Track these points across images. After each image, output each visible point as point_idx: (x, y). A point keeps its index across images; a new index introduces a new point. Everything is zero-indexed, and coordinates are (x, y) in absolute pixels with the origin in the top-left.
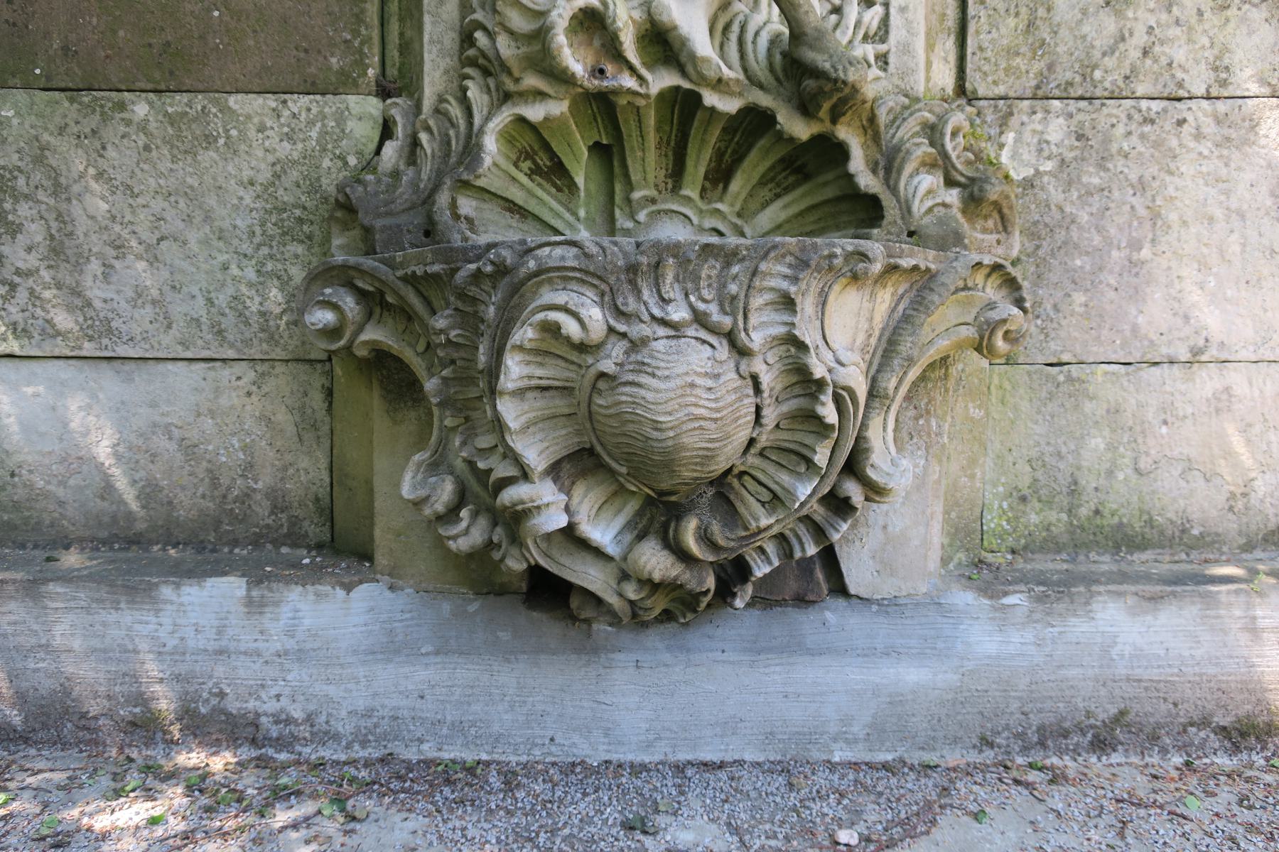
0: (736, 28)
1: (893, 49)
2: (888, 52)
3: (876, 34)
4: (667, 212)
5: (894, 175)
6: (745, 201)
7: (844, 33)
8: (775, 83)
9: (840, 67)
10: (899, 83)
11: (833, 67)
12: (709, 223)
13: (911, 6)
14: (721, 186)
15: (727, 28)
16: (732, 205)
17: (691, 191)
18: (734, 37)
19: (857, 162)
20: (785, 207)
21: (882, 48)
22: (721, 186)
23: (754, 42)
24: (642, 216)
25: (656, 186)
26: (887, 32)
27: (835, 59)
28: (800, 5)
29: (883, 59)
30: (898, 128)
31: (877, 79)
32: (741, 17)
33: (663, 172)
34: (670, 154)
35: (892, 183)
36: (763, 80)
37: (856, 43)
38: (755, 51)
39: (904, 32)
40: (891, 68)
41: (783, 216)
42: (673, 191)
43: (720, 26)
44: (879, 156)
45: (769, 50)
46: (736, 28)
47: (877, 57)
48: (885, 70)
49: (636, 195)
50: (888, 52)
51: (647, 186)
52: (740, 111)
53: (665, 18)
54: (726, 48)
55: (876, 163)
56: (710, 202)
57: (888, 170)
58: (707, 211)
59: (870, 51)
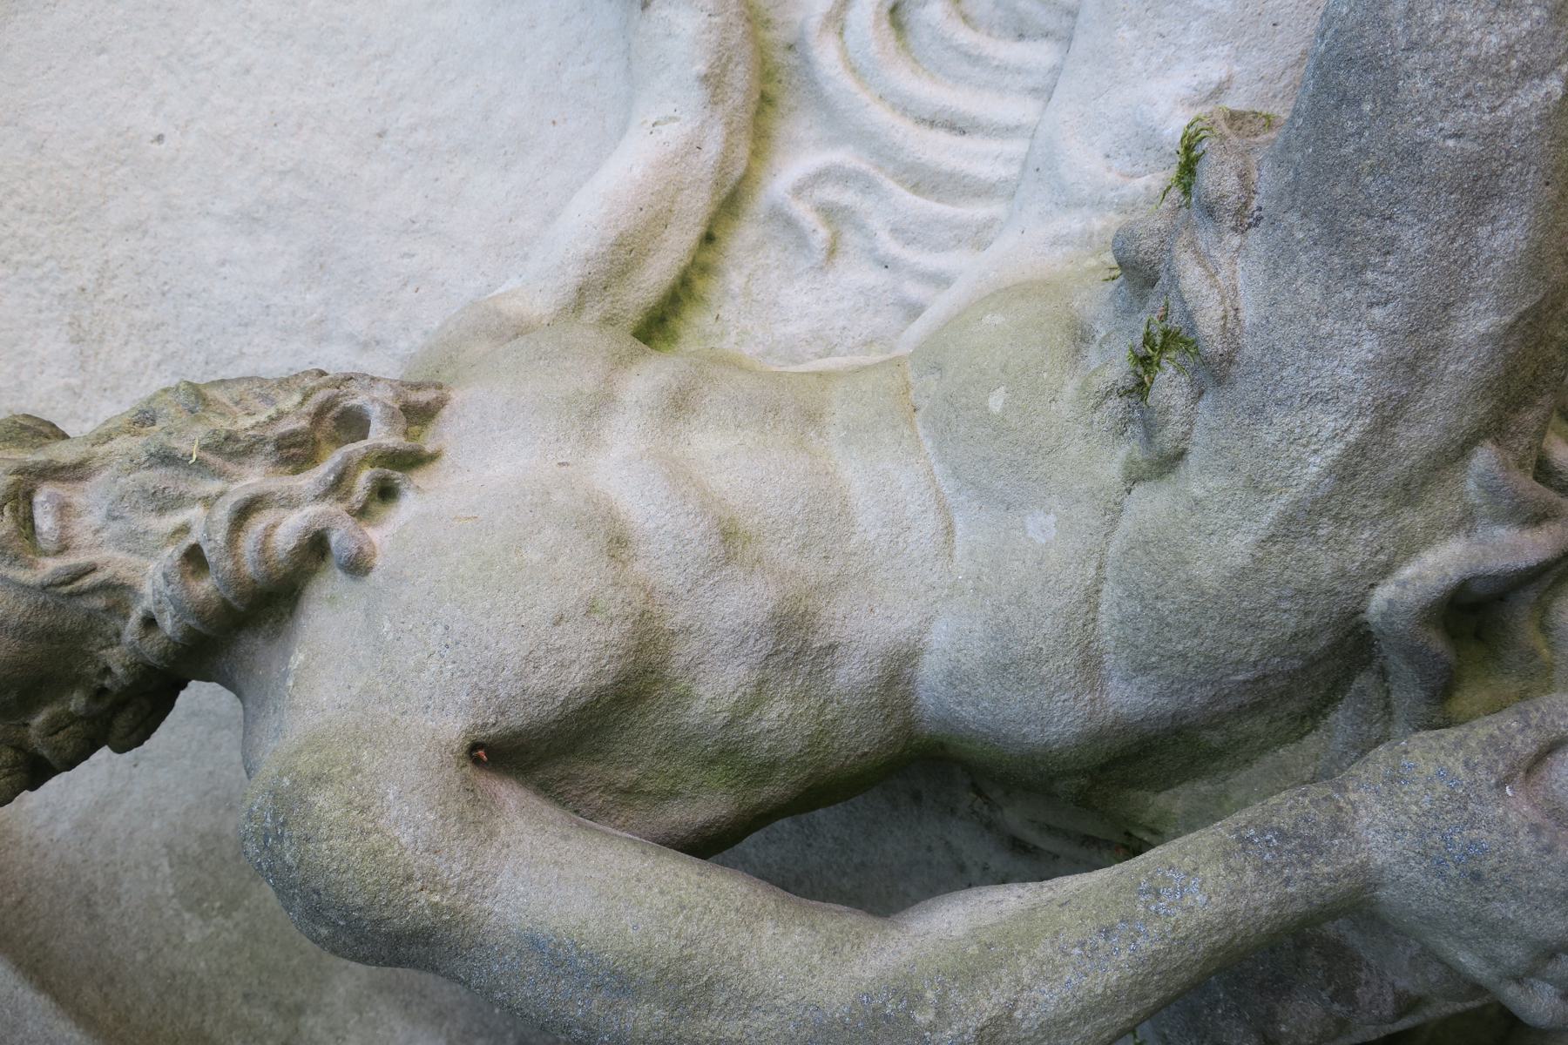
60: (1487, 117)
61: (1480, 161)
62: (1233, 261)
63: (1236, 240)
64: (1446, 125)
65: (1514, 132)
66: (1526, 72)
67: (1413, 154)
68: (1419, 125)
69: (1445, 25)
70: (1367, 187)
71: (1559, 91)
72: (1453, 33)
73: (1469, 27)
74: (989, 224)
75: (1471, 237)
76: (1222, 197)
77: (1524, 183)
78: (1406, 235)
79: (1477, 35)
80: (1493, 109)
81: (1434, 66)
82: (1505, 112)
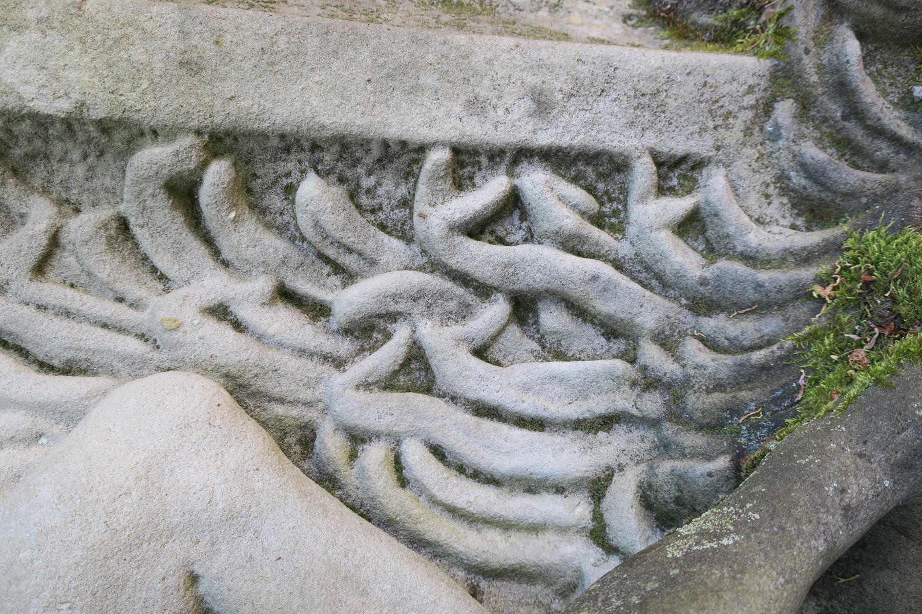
1: (651, 139)
3: (590, 190)
7: (607, 289)
10: (738, 125)
13: (530, 80)
21: (643, 173)
29: (675, 171)
30: (878, 132)
37: (624, 249)
39: (603, 105)
40: (700, 146)
47: (662, 190)
48: (700, 164)
59: (652, 214)
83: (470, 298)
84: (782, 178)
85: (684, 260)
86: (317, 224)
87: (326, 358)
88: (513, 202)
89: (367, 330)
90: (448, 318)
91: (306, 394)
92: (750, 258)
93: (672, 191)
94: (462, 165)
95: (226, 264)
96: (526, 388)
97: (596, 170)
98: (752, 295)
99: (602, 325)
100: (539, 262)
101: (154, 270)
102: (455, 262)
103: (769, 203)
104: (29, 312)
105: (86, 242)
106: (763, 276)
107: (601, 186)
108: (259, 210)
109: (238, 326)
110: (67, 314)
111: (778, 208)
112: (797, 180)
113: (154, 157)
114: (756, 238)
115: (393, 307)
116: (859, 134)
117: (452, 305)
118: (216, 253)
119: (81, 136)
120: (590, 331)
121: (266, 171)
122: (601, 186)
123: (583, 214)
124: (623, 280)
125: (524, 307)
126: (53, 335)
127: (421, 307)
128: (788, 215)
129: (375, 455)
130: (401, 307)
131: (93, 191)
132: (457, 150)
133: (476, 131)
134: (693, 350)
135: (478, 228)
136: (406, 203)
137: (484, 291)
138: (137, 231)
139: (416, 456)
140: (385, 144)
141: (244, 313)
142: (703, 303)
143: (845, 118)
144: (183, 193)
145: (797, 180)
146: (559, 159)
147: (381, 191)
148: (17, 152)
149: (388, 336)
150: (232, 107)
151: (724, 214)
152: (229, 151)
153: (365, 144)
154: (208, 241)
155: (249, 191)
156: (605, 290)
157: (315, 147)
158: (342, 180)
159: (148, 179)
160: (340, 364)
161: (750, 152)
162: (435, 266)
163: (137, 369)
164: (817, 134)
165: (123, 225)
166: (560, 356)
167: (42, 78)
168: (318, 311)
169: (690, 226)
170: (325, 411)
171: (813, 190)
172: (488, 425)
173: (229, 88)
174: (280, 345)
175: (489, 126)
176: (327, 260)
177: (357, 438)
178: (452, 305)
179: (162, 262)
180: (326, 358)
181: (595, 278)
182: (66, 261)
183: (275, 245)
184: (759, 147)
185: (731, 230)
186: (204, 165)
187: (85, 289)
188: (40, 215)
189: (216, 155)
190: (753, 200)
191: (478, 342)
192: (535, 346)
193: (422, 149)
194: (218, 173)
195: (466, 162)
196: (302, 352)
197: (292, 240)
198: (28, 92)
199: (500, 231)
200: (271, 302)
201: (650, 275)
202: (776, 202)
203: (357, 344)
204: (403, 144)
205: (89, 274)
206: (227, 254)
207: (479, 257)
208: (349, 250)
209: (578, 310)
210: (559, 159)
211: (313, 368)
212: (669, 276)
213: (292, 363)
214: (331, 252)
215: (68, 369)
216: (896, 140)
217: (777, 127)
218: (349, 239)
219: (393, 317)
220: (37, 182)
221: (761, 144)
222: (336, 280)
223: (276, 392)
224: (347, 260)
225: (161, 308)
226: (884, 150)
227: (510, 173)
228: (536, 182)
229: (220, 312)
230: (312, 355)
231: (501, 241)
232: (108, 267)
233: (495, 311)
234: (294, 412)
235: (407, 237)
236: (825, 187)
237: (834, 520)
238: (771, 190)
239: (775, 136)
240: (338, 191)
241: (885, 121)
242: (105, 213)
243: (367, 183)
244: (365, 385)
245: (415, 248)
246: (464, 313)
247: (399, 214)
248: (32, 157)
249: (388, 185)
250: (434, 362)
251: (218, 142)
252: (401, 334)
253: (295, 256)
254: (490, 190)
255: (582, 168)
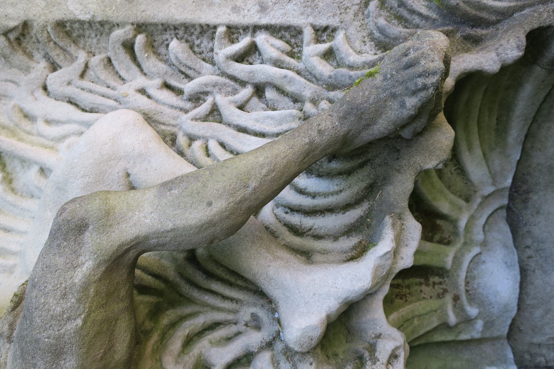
0: (295, 219)
1: (311, 20)
2: (314, 27)
3: (288, 42)
4: (467, 283)
5: (484, 15)
6: (454, 193)
7: (291, 81)
8: (367, 169)
9: (420, 82)
10: (351, 12)
11: (414, 93)
12: (479, 236)
14: (439, 222)
15: (295, 230)
16: (460, 209)
17: (447, 256)
18: (308, 222)
19: (486, 59)
20: (470, 148)
21: (308, 34)
22: (439, 222)
23: (314, 196)
24: (473, 311)
25: (440, 296)
26: (288, 28)
27: (399, 90)
28: (311, 143)
29: (323, 32)
30: (413, 12)
31: (348, 38)
32: (280, 212)
33: (424, 288)
34: (407, 282)
35: (493, 18)
36: (363, 185)
37: (300, 66)
38: (326, 195)
40: (333, 22)
41: (478, 152)
42: (441, 276)
43: (297, 241)
44: (458, 35)
45: (319, 176)
46: (295, 219)
47: (318, 41)
48: (334, 30)
49: (452, 319)
50: (314, 27)
51: (442, 308)
52: (417, 218)
53: (318, 333)
54: (322, 232)
55: (467, 38)
56: (456, 234)
57: (477, 22)
58: (465, 236)
59: (312, 50)
60: (57, 333)
61: (56, 345)
62: (7, 353)
63: (8, 346)
64: (45, 335)
65: (66, 337)
66: (69, 319)
67: (37, 341)
68: (38, 333)
69: (44, 304)
70: (28, 346)
71: (81, 323)
72: (47, 306)
73: (51, 305)
74: (14, 266)
75: (58, 364)
76: (3, 333)
77: (72, 350)
78: (39, 363)
79: (54, 307)
80: (58, 331)
81: (41, 316)
82: (62, 331)
83: (237, 86)
84: (371, 34)
85: (325, 69)
86: (176, 58)
87: (181, 109)
88: (253, 49)
89: (197, 98)
90: (228, 94)
91: (173, 122)
92: (351, 67)
93: (324, 42)
94: (233, 34)
95: (145, 74)
96: (257, 121)
97: (288, 33)
98: (349, 81)
99: (292, 97)
100: (261, 71)
101: (120, 77)
102: (230, 71)
103: (365, 45)
104: (79, 90)
105: (97, 66)
106: (352, 73)
107: (293, 41)
108: (157, 54)
109: (149, 97)
110: (91, 91)
111: (369, 47)
112: (377, 34)
113: (118, 34)
114: (354, 58)
115: (206, 89)
116: (405, 14)
117: (230, 89)
118: (142, 70)
119: (94, 28)
120: (286, 99)
121: (159, 39)
122: (293, 41)
123: (283, 52)
124: (298, 78)
125: (259, 90)
126: (86, 99)
127: (216, 90)
128: (373, 50)
129: (197, 144)
130: (209, 89)
131: (99, 48)
132: (229, 27)
133: (236, 19)
134: (324, 105)
135: (241, 58)
136: (212, 50)
137: (243, 84)
138: (114, 62)
139: (213, 146)
140: (201, 26)
141: (151, 91)
142: (332, 86)
143: (399, 6)
144: (129, 47)
145: (377, 34)
146: (273, 30)
147: (202, 45)
148: (75, 35)
149: (205, 101)
150: (144, 14)
151: (341, 49)
152: (144, 31)
153: (193, 26)
154: (139, 66)
155: (153, 46)
156: (290, 82)
157: (175, 28)
158: (187, 41)
159: (116, 42)
160: (186, 111)
161: (357, 23)
162: (223, 74)
163: (113, 109)
164: (388, 14)
165: (109, 60)
166: (274, 109)
167: (81, 7)
168: (179, 92)
169: (329, 55)
170: (180, 129)
171: (382, 38)
172: (241, 135)
173: (143, 7)
174: (164, 104)
175: (241, 17)
176: (182, 73)
177: (192, 139)
178: (230, 89)
179: (123, 73)
180: (181, 109)
181: (285, 77)
182: (90, 73)
183: (162, 67)
184: (361, 21)
185: (343, 55)
186: (135, 36)
187: (97, 83)
188: (82, 56)
189: (140, 33)
190: (358, 44)
191: (239, 104)
192: (264, 106)
193: (215, 27)
194: (140, 39)
195: (233, 32)
196: (172, 107)
197: (170, 65)
198: (77, 12)
199: (251, 60)
200: (161, 88)
201: (310, 76)
202: (368, 44)
203: (193, 105)
204: (208, 25)
205: (98, 78)
206: (145, 71)
207: (240, 69)
208: (190, 68)
209: (280, 90)
210: (273, 30)
211: (176, 113)
212: (318, 76)
213: (167, 110)
214: (183, 69)
215: (92, 111)
216: (420, 15)
217: (369, 12)
218: (189, 63)
219: (206, 93)
220: (81, 45)
221: (363, 20)
222: (186, 80)
223: (162, 120)
224: (190, 72)
225: (122, 89)
226: (417, 20)
227: (253, 35)
228: (261, 39)
229: (142, 91)
230: (176, 108)
231: (251, 64)
232: (104, 75)
233: (247, 91)
234: (169, 128)
235: (213, 63)
236: (386, 36)
237: (314, 134)
238: (366, 39)
239: (368, 16)
240: (185, 46)
241: (415, 7)
242: (103, 56)
243: (197, 42)
244: (196, 119)
245: (216, 67)
246: (235, 92)
247: (210, 54)
248: (79, 36)
249: (205, 43)
250: (221, 110)
251: (140, 28)
252: (210, 100)
253: (170, 71)
254: (244, 42)
255: (283, 33)
